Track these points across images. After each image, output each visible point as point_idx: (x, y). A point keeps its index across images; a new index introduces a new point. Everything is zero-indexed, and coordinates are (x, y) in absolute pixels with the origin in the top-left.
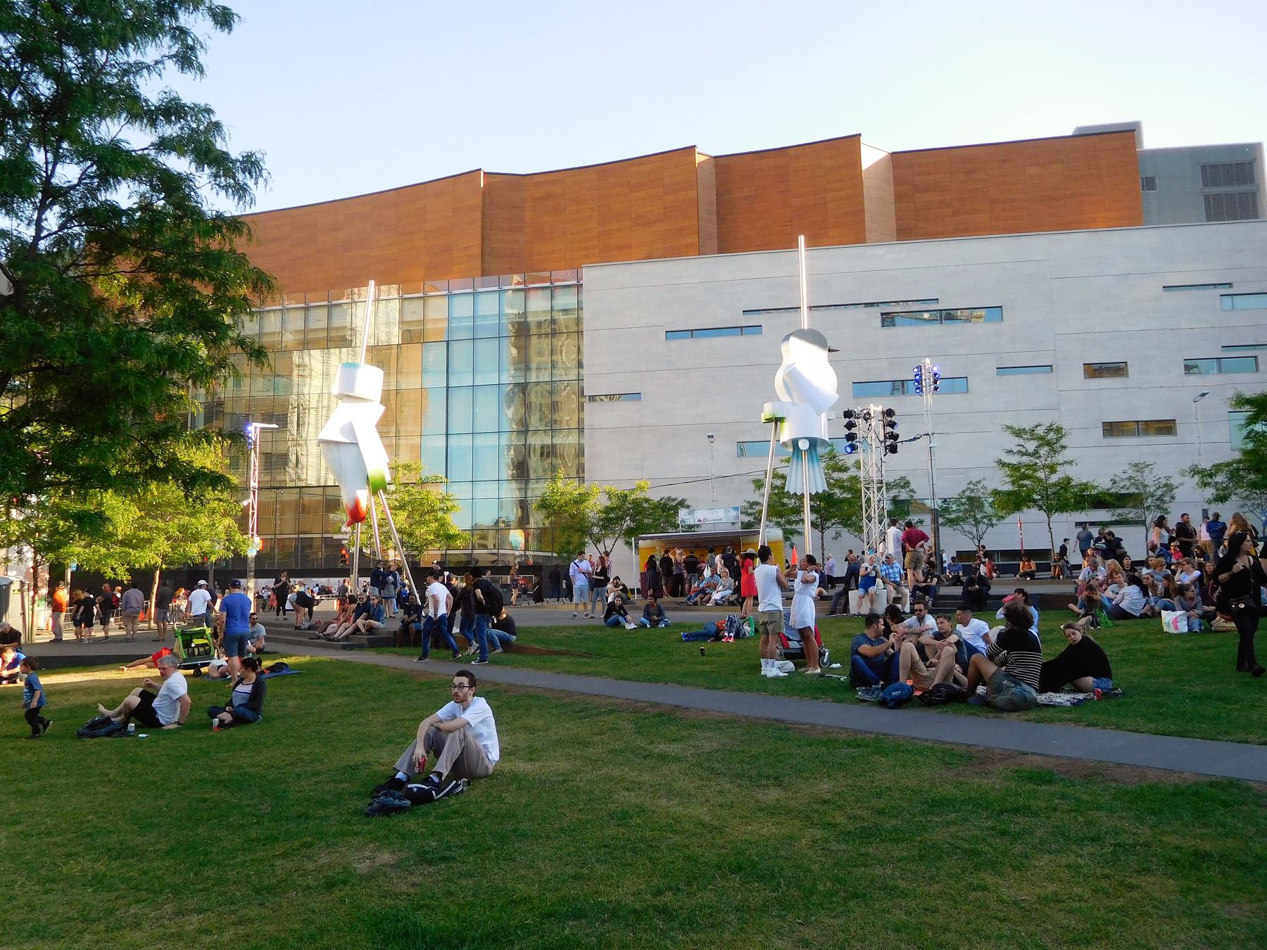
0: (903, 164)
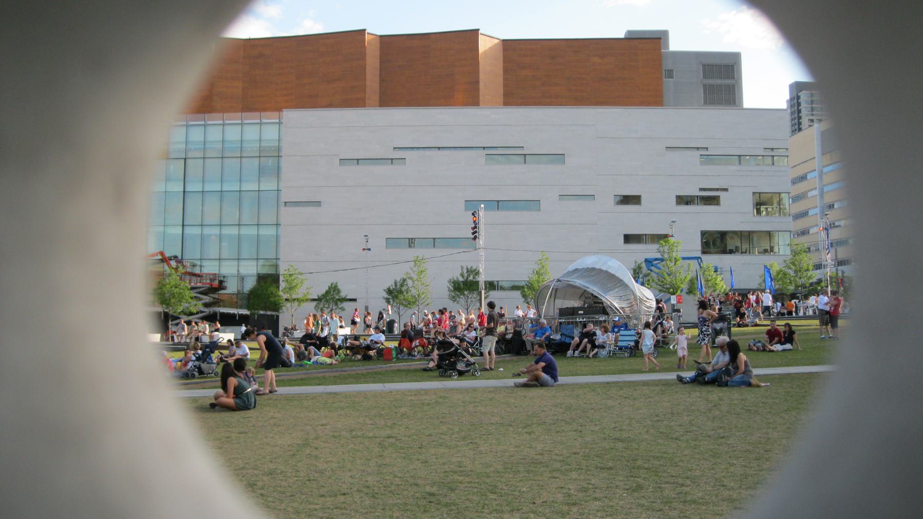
0: (513, 50)
